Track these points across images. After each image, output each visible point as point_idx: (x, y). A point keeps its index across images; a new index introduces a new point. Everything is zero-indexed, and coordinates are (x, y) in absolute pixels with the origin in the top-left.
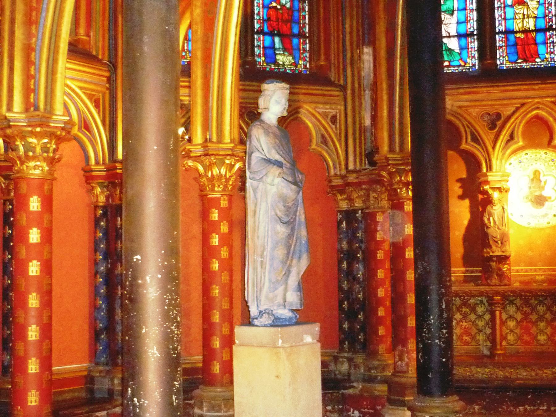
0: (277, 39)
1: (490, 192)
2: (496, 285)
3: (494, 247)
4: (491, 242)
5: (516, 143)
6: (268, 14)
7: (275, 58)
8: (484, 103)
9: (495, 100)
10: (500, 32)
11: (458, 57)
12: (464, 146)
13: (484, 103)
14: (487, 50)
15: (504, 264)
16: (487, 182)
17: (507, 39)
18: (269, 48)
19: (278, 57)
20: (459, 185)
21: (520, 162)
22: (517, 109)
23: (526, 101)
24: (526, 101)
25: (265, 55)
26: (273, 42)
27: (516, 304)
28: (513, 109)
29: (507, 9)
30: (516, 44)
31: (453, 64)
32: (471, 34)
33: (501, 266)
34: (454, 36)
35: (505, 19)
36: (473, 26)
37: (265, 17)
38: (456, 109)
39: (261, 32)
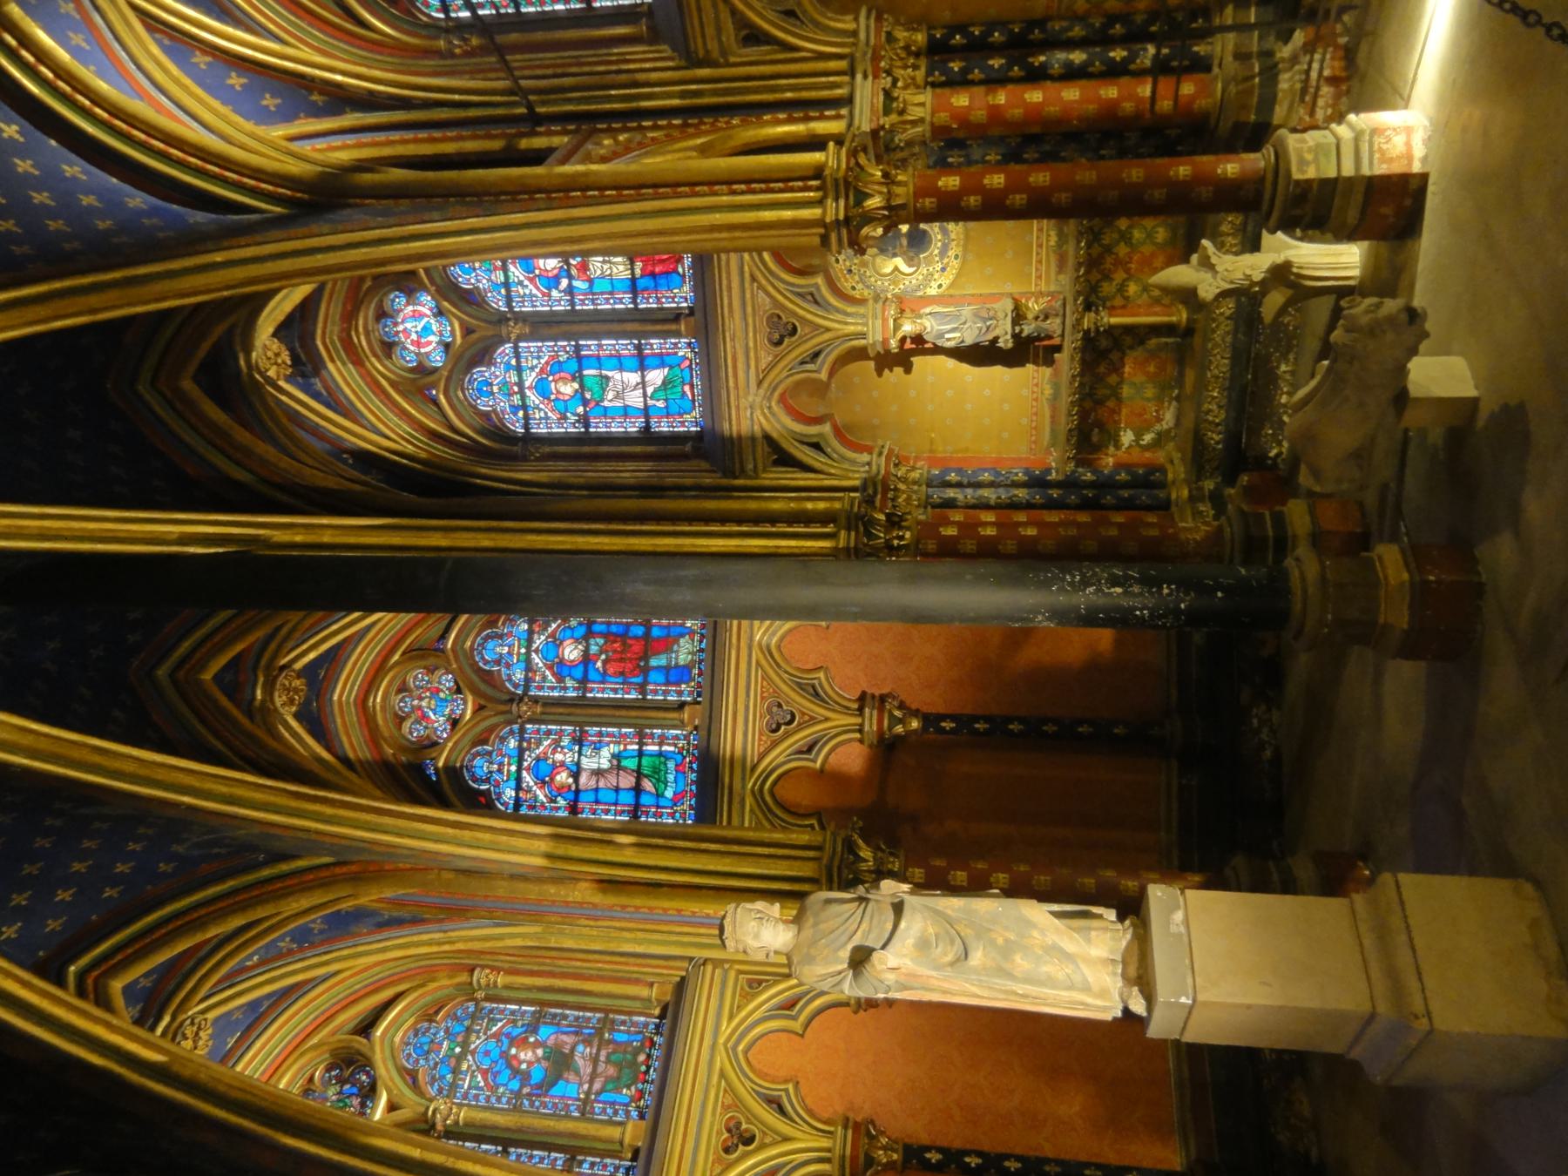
0: (654, 662)
1: (900, 335)
2: (1064, 323)
3: (997, 332)
4: (990, 337)
5: (818, 288)
6: (615, 675)
7: (684, 667)
8: (751, 344)
9: (747, 325)
10: (634, 301)
11: (677, 370)
12: (824, 376)
13: (751, 344)
14: (666, 321)
15: (1027, 308)
16: (885, 341)
17: (645, 289)
18: (667, 677)
19: (682, 663)
20: (886, 371)
21: (850, 271)
22: (761, 287)
23: (747, 275)
24: (747, 275)
25: (678, 684)
26: (658, 668)
27: (1098, 281)
28: (761, 293)
29: (596, 289)
30: (653, 275)
31: (687, 379)
32: (639, 347)
33: (1030, 316)
34: (643, 377)
35: (611, 293)
36: (625, 346)
37: (620, 680)
38: (762, 391)
39: (642, 689)
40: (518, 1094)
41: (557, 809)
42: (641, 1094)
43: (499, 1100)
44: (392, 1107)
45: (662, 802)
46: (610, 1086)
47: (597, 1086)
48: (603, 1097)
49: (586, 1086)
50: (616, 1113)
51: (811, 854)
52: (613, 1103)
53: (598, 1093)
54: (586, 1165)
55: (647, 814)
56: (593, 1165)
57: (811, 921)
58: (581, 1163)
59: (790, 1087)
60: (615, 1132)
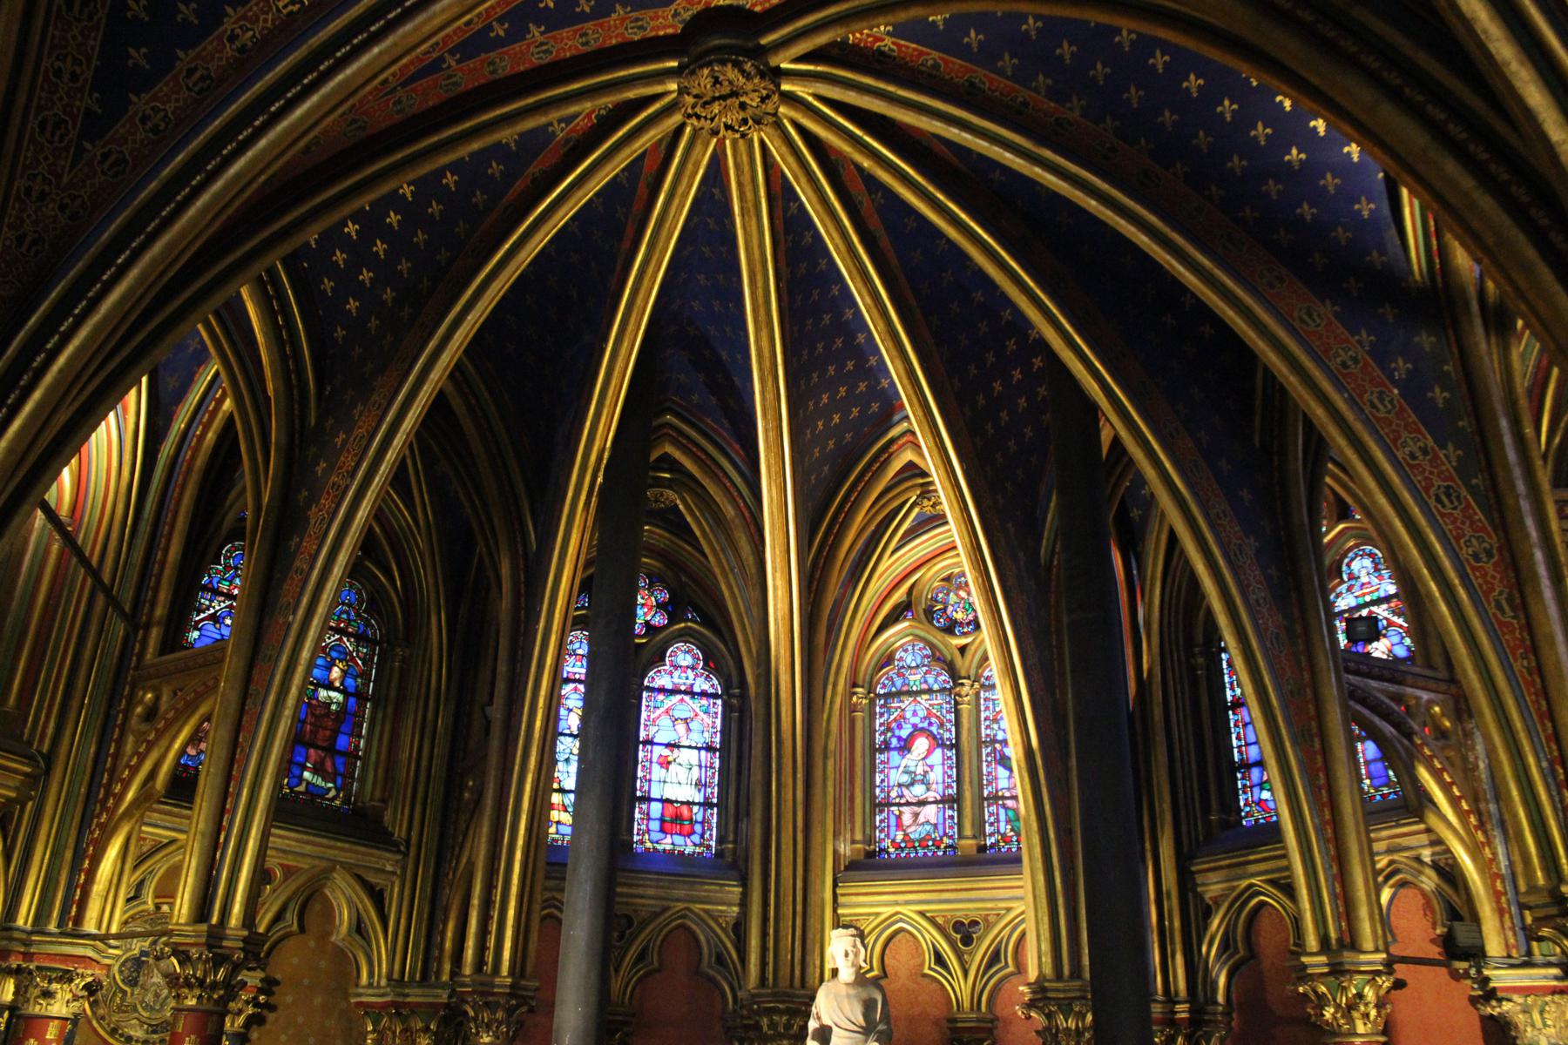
40: (994, 741)
41: (1232, 689)
42: (1007, 840)
43: (988, 727)
44: (963, 650)
45: (1256, 790)
46: (1011, 814)
47: (1009, 803)
48: (1002, 811)
49: (1007, 794)
50: (992, 824)
51: (1066, 971)
52: (998, 821)
53: (1004, 806)
54: (949, 812)
55: (1243, 778)
56: (952, 817)
57: (852, 991)
58: (951, 808)
59: (1011, 969)
60: (968, 832)
